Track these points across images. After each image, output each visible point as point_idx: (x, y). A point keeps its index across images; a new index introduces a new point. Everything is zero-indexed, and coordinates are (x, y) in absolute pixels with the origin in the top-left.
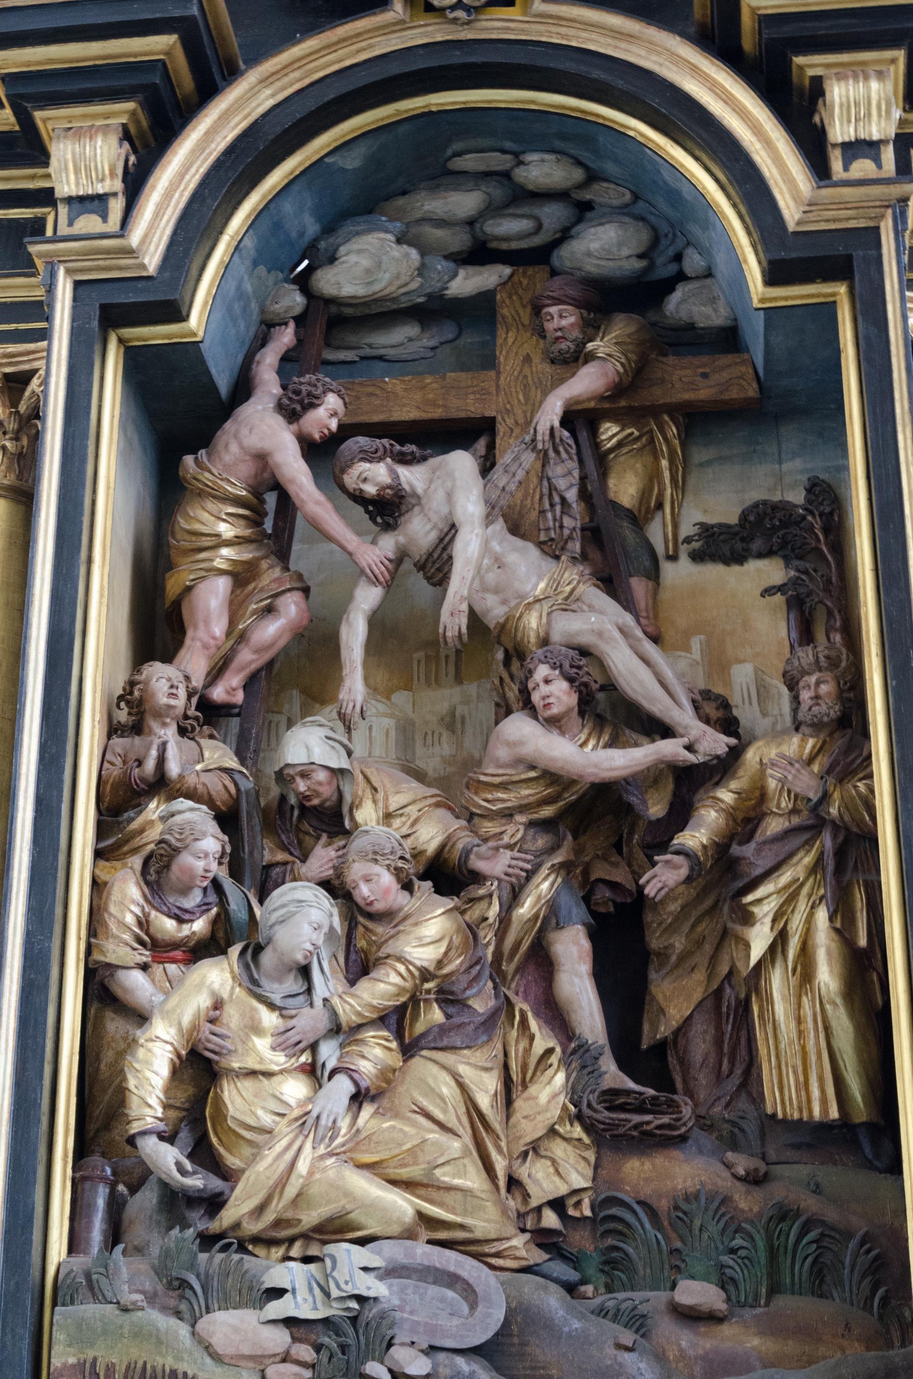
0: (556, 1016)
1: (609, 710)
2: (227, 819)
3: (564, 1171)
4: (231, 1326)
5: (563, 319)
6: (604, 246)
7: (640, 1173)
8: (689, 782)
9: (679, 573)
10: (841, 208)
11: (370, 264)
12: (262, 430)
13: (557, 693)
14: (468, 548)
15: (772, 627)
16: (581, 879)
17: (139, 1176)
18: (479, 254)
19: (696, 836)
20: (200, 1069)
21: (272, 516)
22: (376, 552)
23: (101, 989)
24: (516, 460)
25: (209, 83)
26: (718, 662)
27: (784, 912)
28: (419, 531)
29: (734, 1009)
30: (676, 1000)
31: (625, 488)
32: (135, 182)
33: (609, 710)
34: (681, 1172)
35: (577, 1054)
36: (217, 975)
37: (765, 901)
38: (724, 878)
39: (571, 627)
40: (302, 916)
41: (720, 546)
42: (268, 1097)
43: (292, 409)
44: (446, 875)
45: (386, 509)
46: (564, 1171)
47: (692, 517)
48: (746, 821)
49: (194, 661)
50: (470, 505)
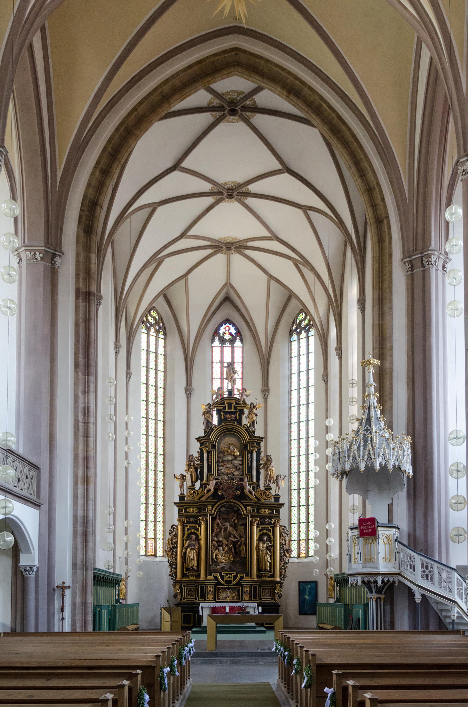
0: (232, 552)
1: (235, 537)
2: (216, 542)
3: (232, 559)
4: (218, 567)
5: (233, 513)
6: (235, 509)
7: (235, 559)
8: (238, 541)
9: (239, 527)
10: (247, 514)
11: (223, 509)
12: (218, 521)
13: (232, 536)
14: (228, 529)
15: (243, 530)
16: (233, 545)
17: (213, 559)
18: (228, 508)
19: (239, 544)
20: (216, 555)
21: (218, 524)
22: (223, 527)
23: (212, 551)
24: (231, 523)
25: (215, 504)
26: (240, 532)
27: (243, 547)
28: (226, 526)
29: (240, 551)
30: (237, 550)
31: (236, 521)
32: (212, 509)
33: (235, 537)
34: (238, 559)
35: (233, 554)
36: (217, 551)
37: (242, 547)
38: (240, 546)
39: (234, 533)
40: (221, 548)
41: (241, 525)
42: (219, 556)
43: (219, 519)
44: (227, 545)
45: (225, 525)
46: (232, 559)
47: (240, 523)
48: (241, 543)
49: (214, 533)
50: (228, 526)
